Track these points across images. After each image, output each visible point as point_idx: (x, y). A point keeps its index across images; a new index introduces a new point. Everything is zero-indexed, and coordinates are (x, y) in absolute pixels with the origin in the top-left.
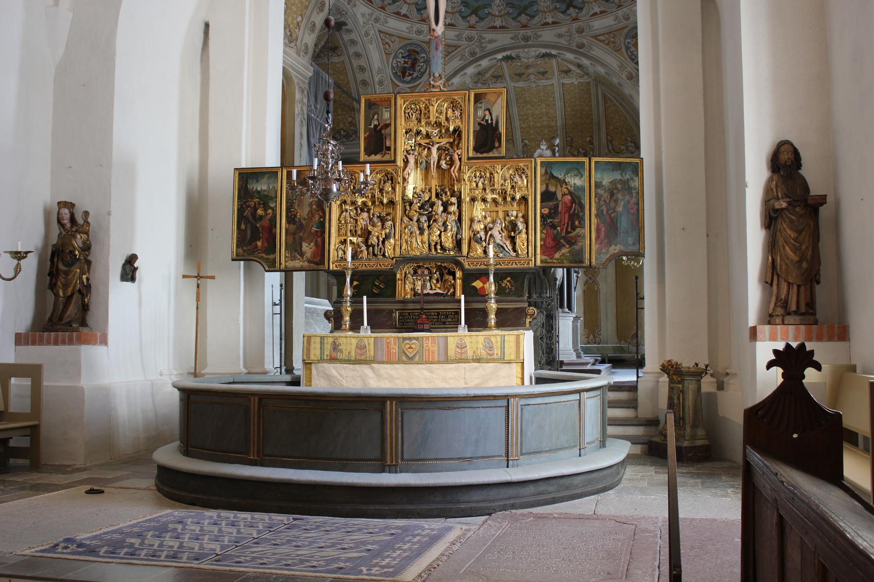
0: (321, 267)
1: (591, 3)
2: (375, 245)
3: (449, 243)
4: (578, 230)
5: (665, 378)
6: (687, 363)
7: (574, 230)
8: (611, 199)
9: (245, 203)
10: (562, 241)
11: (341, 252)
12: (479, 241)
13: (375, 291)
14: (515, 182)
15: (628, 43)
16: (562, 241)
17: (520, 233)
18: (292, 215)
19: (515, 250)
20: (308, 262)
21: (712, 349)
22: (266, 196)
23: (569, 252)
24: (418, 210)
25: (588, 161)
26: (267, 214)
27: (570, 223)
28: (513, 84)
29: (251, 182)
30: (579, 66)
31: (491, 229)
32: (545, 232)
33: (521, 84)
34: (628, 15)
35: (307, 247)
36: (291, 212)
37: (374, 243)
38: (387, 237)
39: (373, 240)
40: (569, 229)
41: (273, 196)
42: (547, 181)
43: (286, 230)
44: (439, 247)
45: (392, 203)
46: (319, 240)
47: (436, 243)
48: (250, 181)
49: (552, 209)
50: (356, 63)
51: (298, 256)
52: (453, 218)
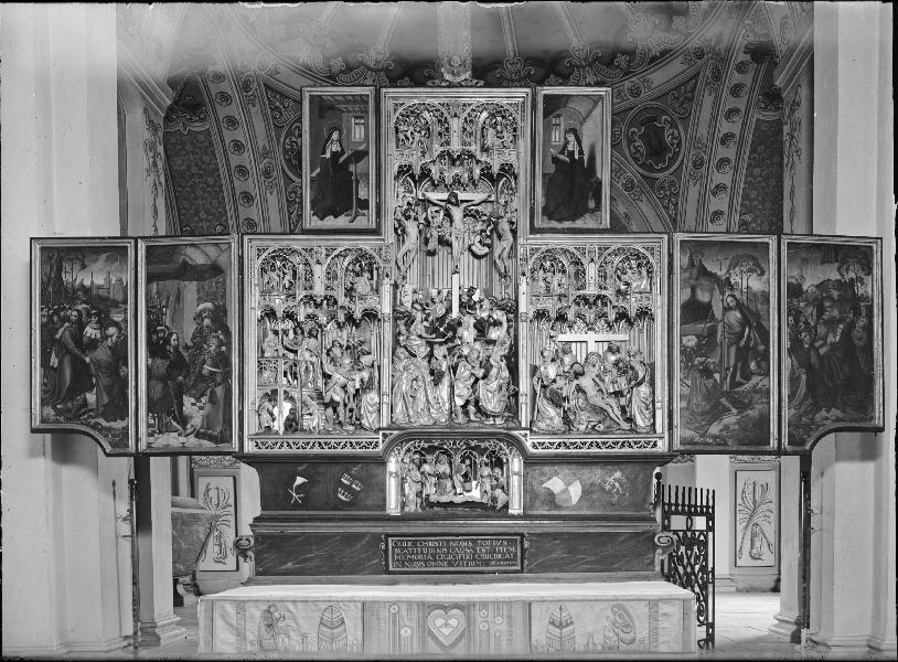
0: (223, 447)
1: (583, 67)
2: (338, 403)
3: (492, 403)
4: (755, 380)
7: (748, 379)
8: (820, 315)
9: (56, 312)
10: (723, 400)
11: (265, 416)
12: (557, 400)
13: (343, 498)
14: (627, 284)
15: (633, 133)
16: (723, 400)
17: (639, 384)
18: (159, 339)
19: (630, 420)
20: (196, 436)
22: (102, 299)
23: (738, 423)
24: (424, 335)
25: (776, 242)
26: (105, 337)
27: (739, 364)
29: (68, 269)
31: (578, 375)
32: (689, 382)
34: (638, 88)
35: (193, 404)
36: (157, 332)
37: (337, 398)
38: (366, 386)
40: (738, 378)
41: (119, 298)
42: (692, 282)
43: (149, 370)
44: (472, 408)
45: (371, 315)
46: (219, 391)
47: (467, 402)
48: (67, 266)
49: (705, 337)
50: (229, 136)
51: (174, 423)
52: (497, 354)
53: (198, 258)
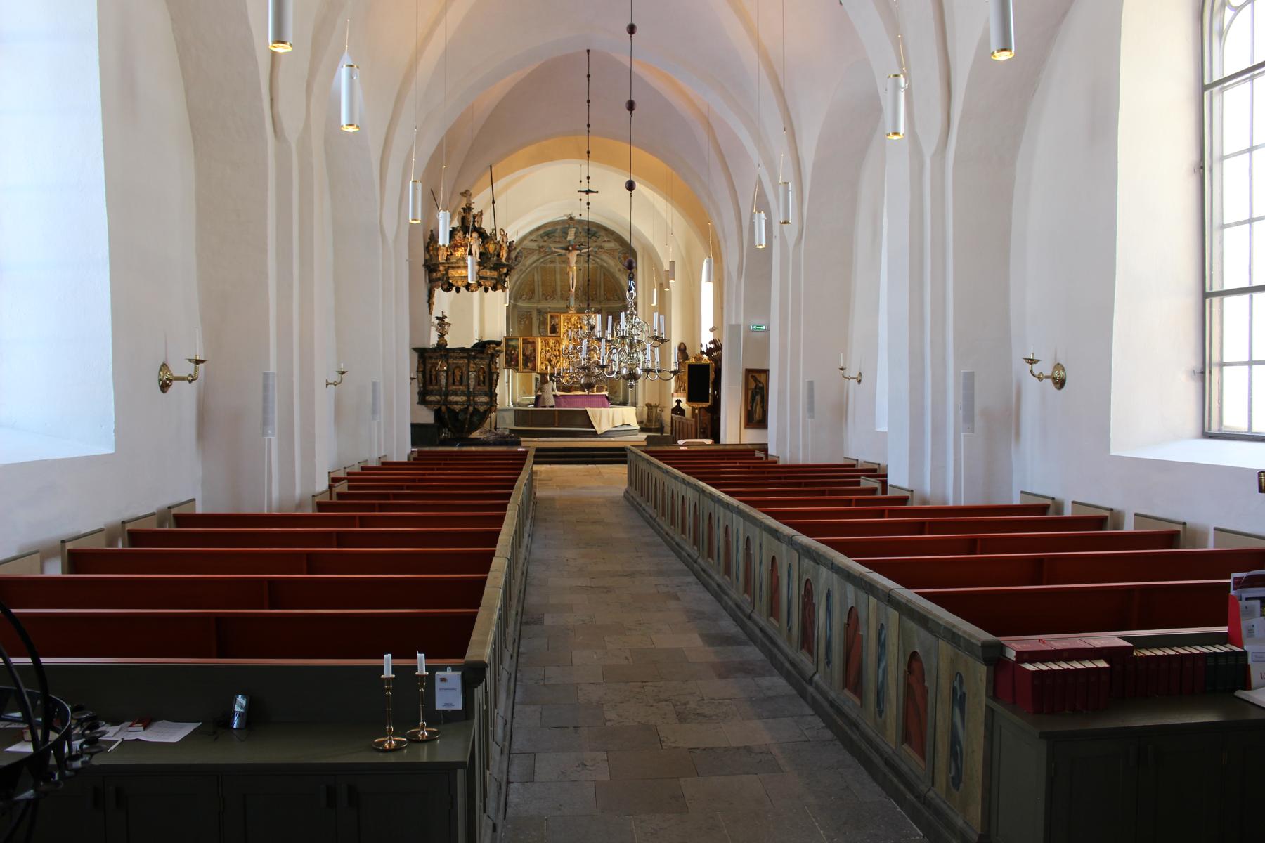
5: (646, 408)
6: (653, 404)
21: (660, 400)
28: (559, 265)
30: (594, 260)
33: (563, 265)
38: (558, 362)
39: (553, 363)
53: (531, 341)
